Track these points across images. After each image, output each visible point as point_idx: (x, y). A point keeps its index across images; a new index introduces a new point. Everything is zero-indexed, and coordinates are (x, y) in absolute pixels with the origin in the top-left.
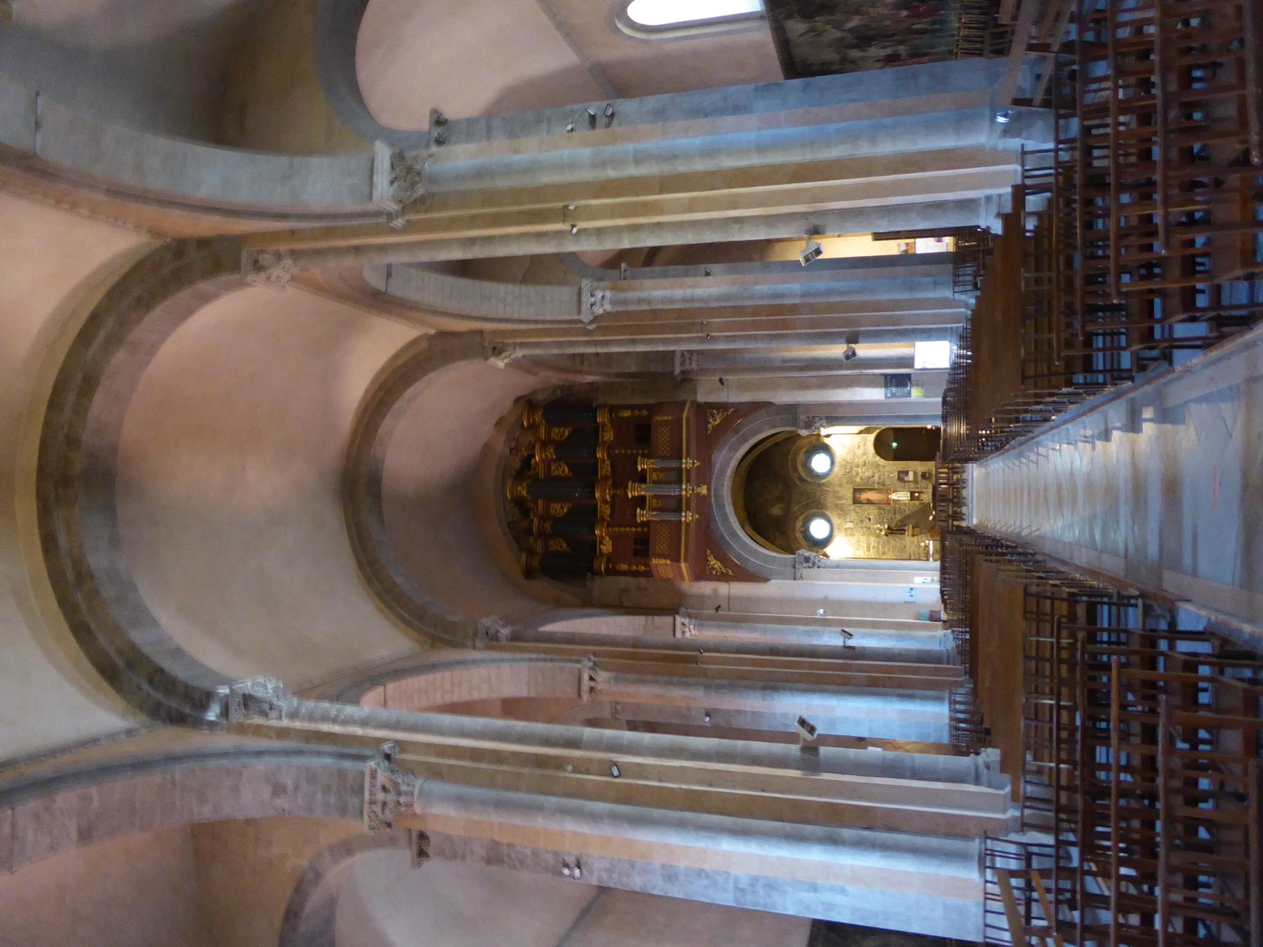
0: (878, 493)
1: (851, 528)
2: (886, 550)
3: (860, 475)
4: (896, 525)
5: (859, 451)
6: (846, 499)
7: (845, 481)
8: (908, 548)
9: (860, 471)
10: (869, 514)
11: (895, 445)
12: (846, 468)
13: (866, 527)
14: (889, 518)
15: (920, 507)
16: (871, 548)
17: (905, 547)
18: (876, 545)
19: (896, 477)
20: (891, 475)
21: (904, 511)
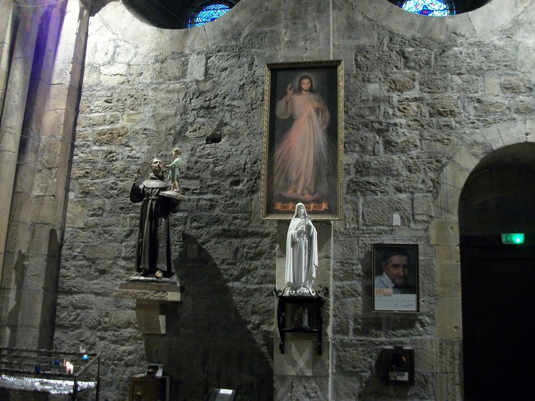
0: (317, 164)
1: (184, 75)
2: (97, 202)
3: (395, 97)
4: (186, 237)
5: (497, 89)
6: (291, 43)
7: (364, 41)
8: (97, 284)
9: (407, 94)
10: (235, 135)
11: (518, 239)
12: (415, 42)
13: (184, 128)
14: (217, 211)
15: (260, 340)
16: (105, 148)
17: (102, 272)
18: (119, 165)
19: (387, 240)
20: (396, 219)
21: (245, 272)
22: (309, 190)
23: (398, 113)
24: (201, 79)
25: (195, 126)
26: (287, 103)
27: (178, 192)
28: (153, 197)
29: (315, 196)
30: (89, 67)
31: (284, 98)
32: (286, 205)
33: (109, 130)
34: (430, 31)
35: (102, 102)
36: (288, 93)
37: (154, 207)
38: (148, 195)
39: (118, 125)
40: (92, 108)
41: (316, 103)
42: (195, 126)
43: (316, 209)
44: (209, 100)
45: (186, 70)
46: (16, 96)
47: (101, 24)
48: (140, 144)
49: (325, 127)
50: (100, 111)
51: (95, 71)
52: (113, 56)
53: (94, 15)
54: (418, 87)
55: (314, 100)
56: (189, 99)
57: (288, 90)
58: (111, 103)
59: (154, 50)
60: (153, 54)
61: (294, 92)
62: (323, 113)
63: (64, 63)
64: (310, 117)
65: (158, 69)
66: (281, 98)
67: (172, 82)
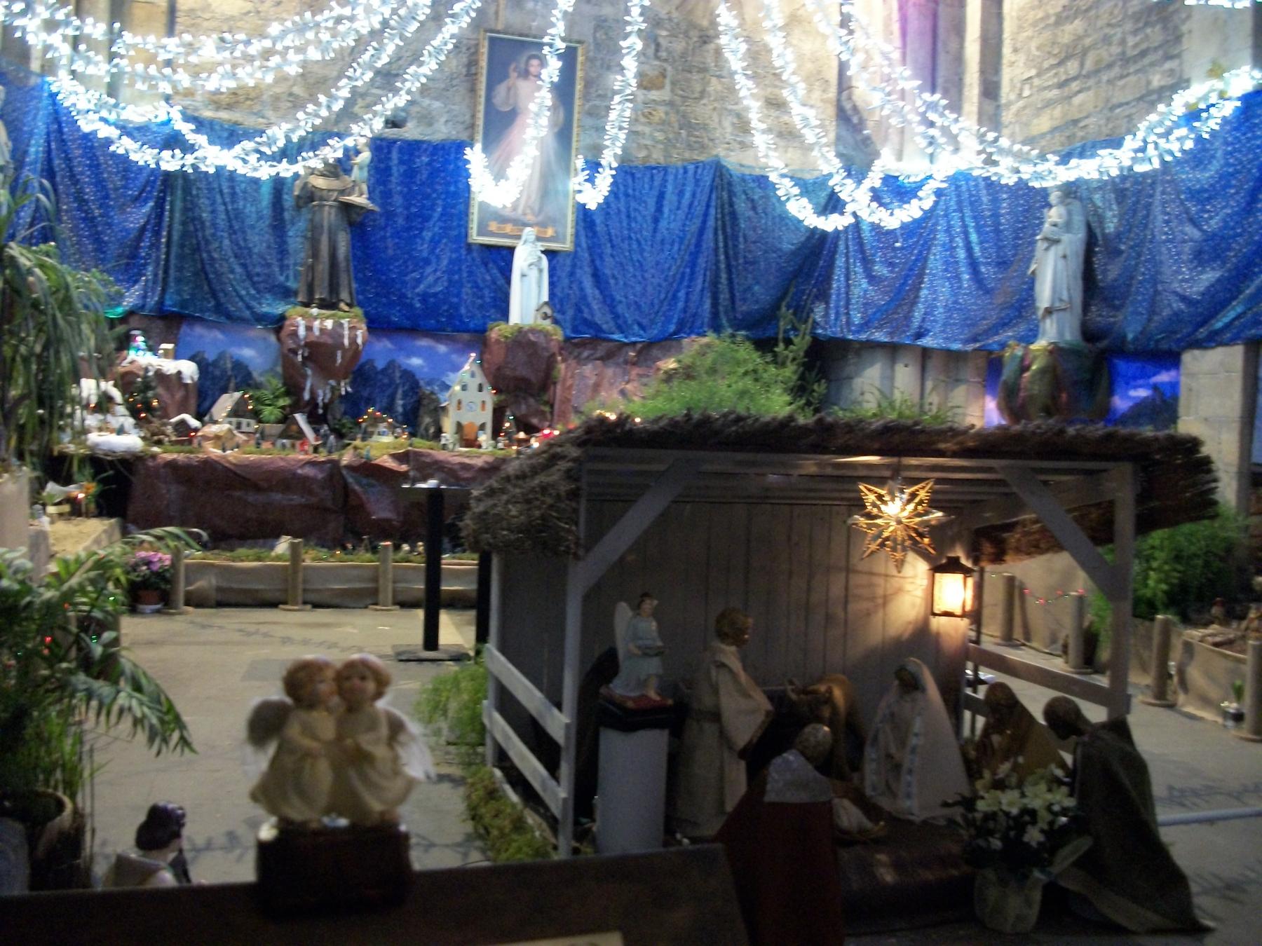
23: (643, 120)
26: (509, 89)
29: (540, 218)
34: (691, 12)
38: (322, 199)
54: (668, 87)
61: (520, 76)
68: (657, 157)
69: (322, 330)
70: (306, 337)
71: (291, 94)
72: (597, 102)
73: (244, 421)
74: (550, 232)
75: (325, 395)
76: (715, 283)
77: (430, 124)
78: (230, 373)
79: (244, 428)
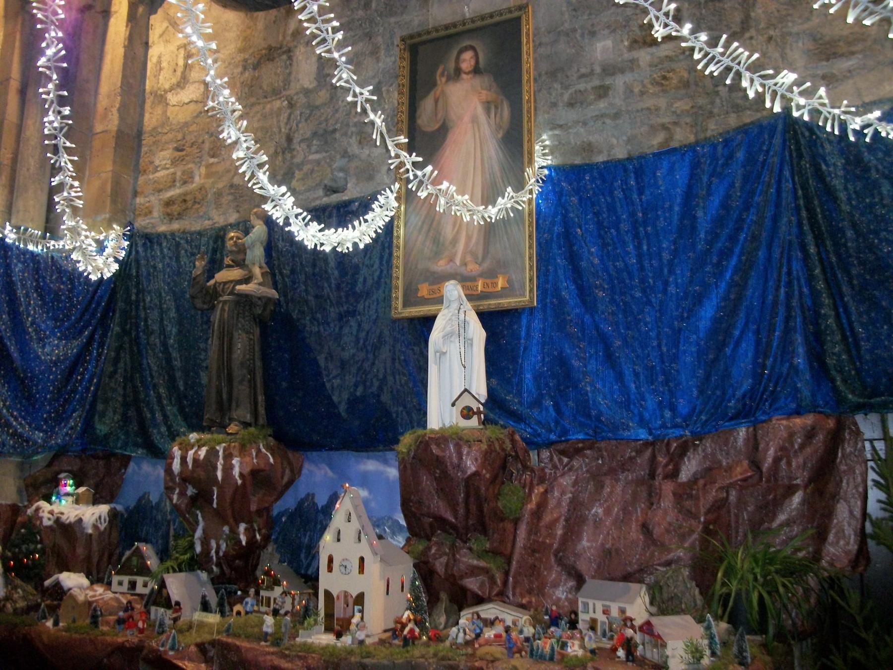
22: (474, 254)
24: (311, 87)
25: (306, 168)
26: (436, 101)
27: (260, 284)
28: (226, 298)
29: (486, 265)
30: (152, 98)
31: (432, 94)
32: (436, 287)
33: (180, 195)
35: (170, 151)
36: (439, 82)
37: (226, 315)
39: (194, 185)
40: (157, 163)
41: (484, 92)
42: (306, 168)
43: (487, 290)
44: (326, 120)
45: (290, 74)
46: (32, 162)
47: (166, 24)
48: (224, 214)
49: (500, 136)
50: (168, 166)
51: (160, 102)
52: (183, 73)
53: (155, 12)
55: (482, 89)
56: (294, 125)
57: (438, 78)
58: (182, 150)
59: (242, 50)
60: (240, 57)
61: (449, 79)
62: (496, 108)
63: (109, 96)
64: (474, 120)
65: (249, 82)
66: (428, 92)
67: (269, 99)
68: (682, 136)
69: (195, 460)
70: (181, 473)
71: (232, 186)
72: (581, 86)
73: (140, 580)
74: (501, 283)
75: (218, 547)
76: (814, 318)
77: (371, 178)
78: (169, 517)
79: (140, 589)
